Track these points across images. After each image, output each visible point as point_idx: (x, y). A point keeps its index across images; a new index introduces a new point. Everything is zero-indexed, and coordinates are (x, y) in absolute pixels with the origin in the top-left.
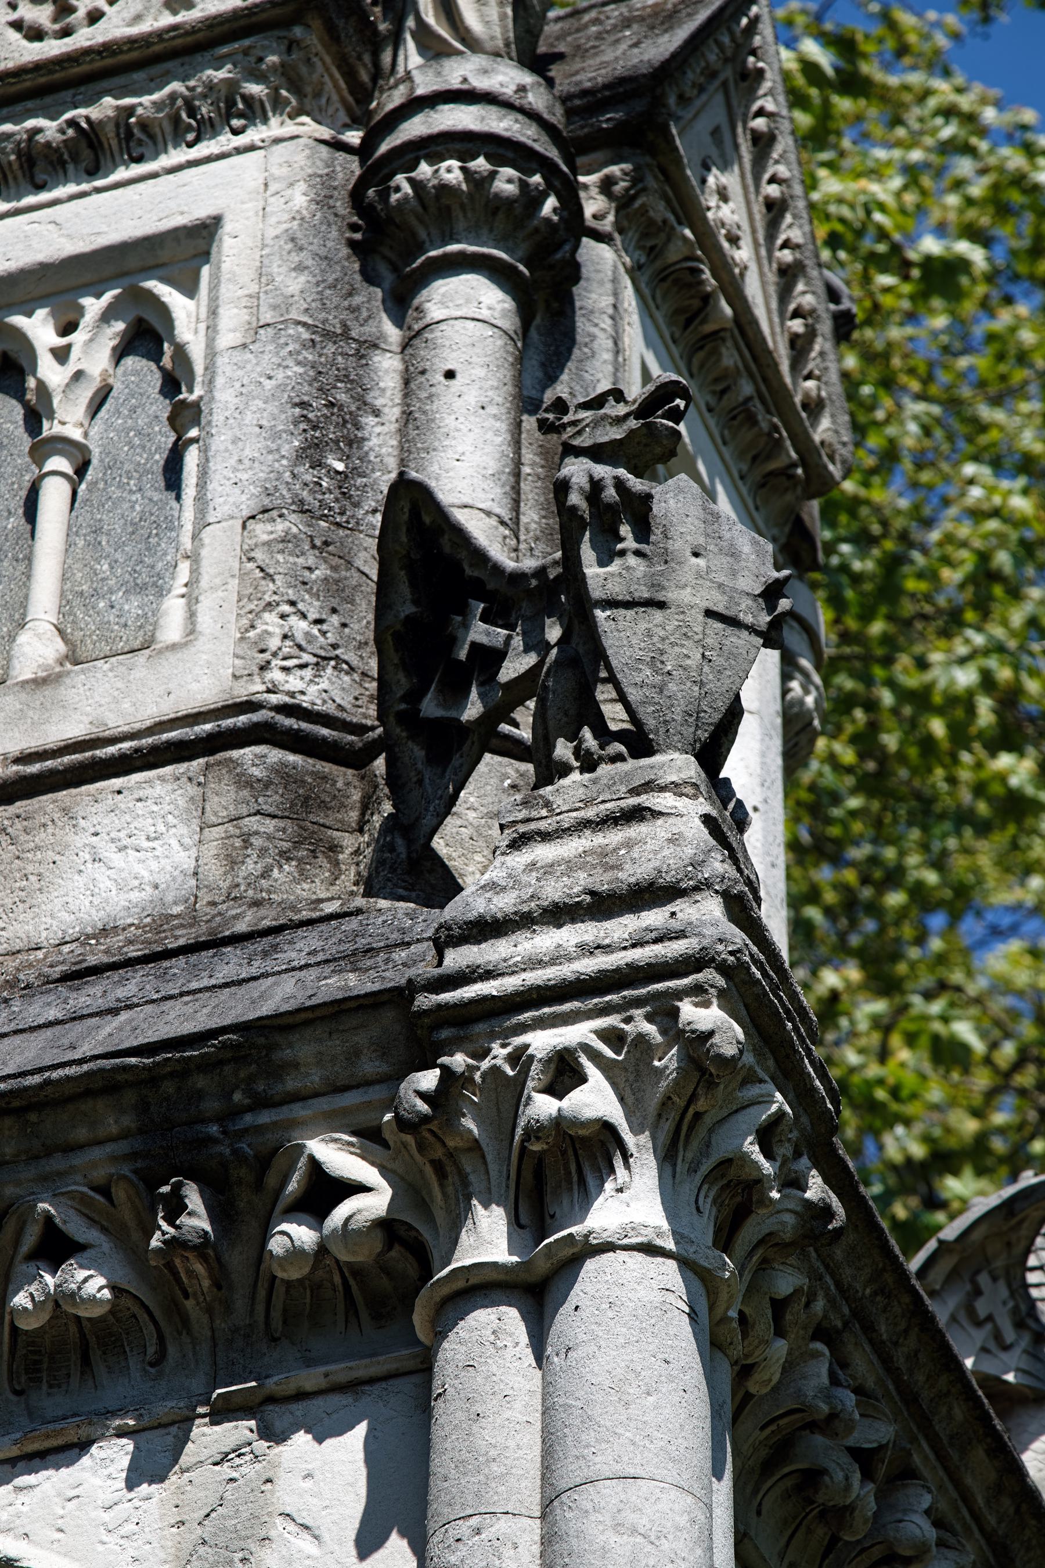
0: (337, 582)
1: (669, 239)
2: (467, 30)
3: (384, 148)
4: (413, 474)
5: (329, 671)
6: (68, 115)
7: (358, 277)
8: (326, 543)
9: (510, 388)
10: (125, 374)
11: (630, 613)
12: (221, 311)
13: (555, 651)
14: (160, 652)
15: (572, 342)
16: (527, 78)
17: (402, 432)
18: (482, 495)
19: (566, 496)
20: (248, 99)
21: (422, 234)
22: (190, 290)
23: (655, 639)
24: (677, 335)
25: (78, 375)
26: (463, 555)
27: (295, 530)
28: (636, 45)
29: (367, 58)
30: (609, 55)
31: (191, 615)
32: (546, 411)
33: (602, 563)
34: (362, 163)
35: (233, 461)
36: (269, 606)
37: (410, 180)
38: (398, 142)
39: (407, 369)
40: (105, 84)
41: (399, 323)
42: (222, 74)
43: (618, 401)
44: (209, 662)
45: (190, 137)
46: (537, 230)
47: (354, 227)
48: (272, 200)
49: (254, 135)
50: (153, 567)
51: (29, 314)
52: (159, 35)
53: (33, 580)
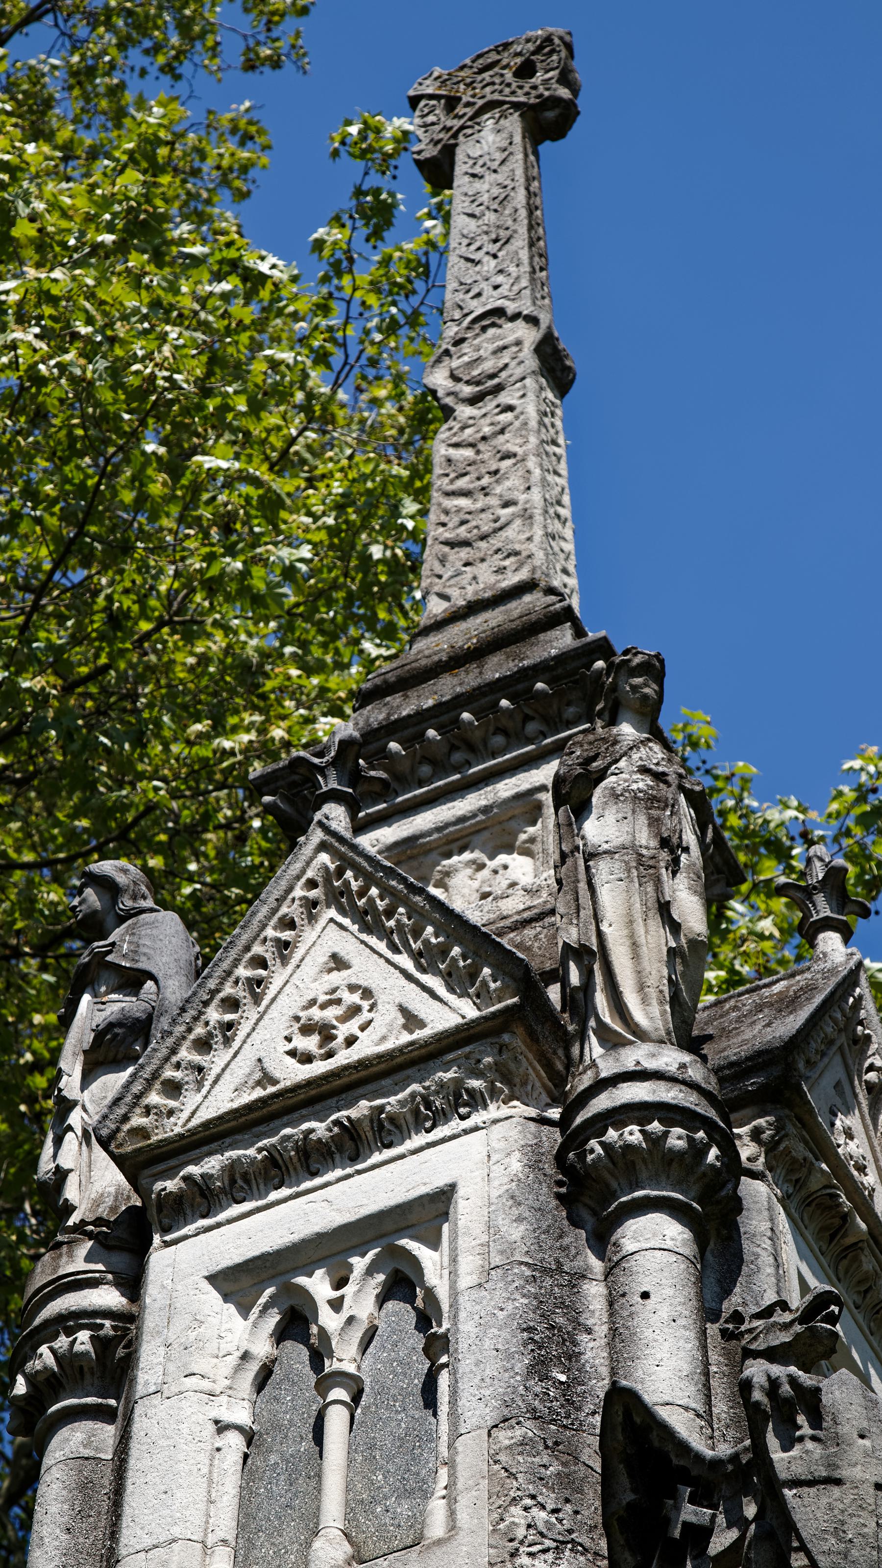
0: (568, 1475)
1: (810, 1173)
2: (637, 1025)
3: (579, 1120)
4: (624, 1383)
5: (567, 1553)
6: (333, 1117)
7: (566, 1222)
8: (557, 1443)
9: (694, 1303)
10: (387, 1315)
11: (813, 1491)
12: (460, 1258)
13: (753, 1526)
14: (428, 1547)
15: (742, 1260)
16: (686, 1058)
17: (611, 1345)
18: (680, 1394)
19: (750, 1394)
20: (471, 1092)
21: (614, 1185)
22: (434, 1243)
23: (836, 1512)
24: (824, 1248)
25: (351, 1320)
26: (670, 1447)
27: (530, 1434)
28: (768, 1025)
29: (560, 1052)
30: (748, 1034)
31: (452, 1514)
32: (726, 1322)
33: (785, 1448)
34: (563, 1133)
35: (477, 1381)
36: (514, 1501)
37: (600, 1143)
38: (590, 1114)
39: (610, 1294)
40: (360, 1091)
41: (601, 1256)
42: (450, 1075)
43: (784, 1310)
44: (468, 1553)
45: (428, 1124)
46: (704, 1174)
47: (560, 1184)
48: (494, 1168)
49: (476, 1119)
50: (418, 1474)
51: (310, 1275)
52: (401, 1050)
53: (323, 1493)
